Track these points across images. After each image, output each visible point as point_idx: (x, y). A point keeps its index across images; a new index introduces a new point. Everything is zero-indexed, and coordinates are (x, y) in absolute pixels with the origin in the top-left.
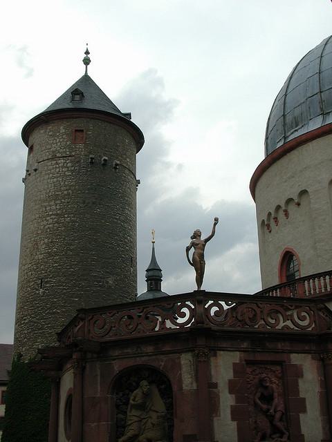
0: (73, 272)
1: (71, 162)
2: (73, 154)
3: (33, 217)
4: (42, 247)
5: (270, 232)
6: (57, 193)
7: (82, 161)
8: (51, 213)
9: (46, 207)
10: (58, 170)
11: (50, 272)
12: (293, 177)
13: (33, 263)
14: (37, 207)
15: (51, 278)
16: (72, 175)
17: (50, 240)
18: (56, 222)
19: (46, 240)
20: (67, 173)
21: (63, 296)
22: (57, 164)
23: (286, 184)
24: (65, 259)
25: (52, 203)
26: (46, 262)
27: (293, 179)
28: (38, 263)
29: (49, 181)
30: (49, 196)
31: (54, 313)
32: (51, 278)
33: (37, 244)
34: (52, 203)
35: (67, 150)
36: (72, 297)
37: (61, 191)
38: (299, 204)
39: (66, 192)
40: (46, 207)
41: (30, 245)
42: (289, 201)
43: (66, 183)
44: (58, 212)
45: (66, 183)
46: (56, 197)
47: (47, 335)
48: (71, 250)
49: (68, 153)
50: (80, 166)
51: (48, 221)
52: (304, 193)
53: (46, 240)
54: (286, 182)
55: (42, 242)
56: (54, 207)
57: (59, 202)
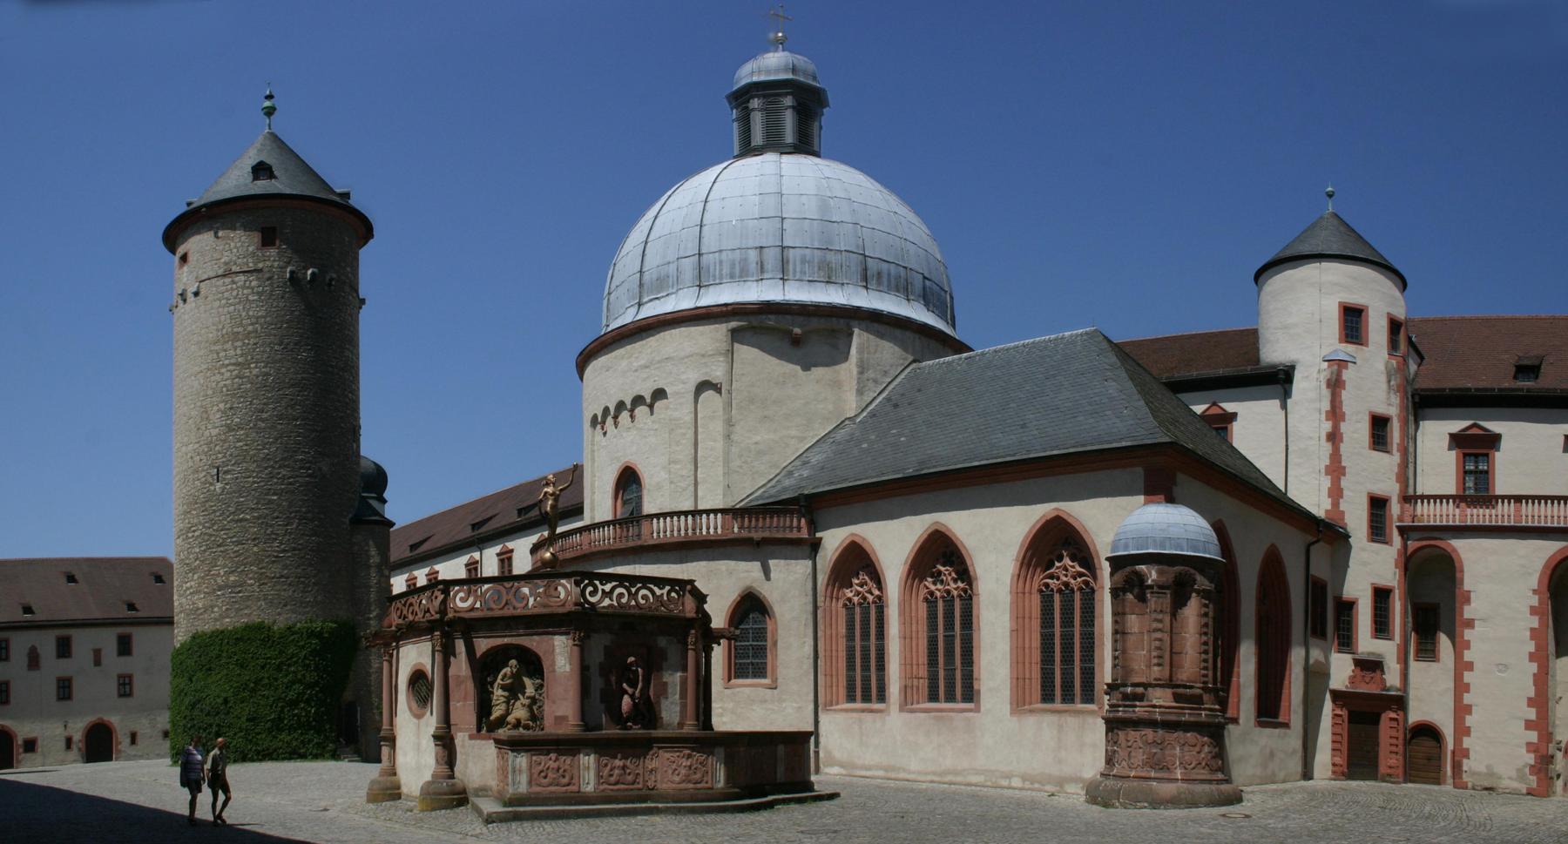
0: (268, 455)
1: (258, 279)
2: (260, 265)
3: (197, 369)
4: (216, 417)
5: (605, 434)
6: (235, 330)
7: (276, 277)
8: (227, 362)
9: (218, 353)
10: (235, 293)
11: (231, 455)
12: (647, 367)
13: (202, 443)
14: (202, 353)
15: (233, 465)
16: (259, 300)
17: (228, 406)
18: (237, 377)
19: (222, 406)
20: (251, 298)
21: (253, 492)
22: (233, 282)
23: (637, 374)
24: (254, 434)
25: (229, 345)
26: (224, 441)
27: (647, 370)
28: (211, 442)
29: (220, 310)
30: (223, 336)
31: (241, 520)
32: (233, 465)
33: (207, 412)
34: (229, 345)
35: (250, 260)
36: (267, 494)
37: (241, 325)
38: (651, 406)
39: (250, 328)
40: (218, 353)
41: (194, 413)
42: (638, 400)
43: (251, 313)
44: (240, 360)
45: (251, 313)
46: (235, 337)
47: (232, 555)
48: (263, 420)
49: (251, 265)
50: (271, 285)
51: (223, 374)
52: (660, 394)
53: (222, 406)
54: (636, 371)
55: (215, 408)
56: (232, 353)
57: (239, 344)
